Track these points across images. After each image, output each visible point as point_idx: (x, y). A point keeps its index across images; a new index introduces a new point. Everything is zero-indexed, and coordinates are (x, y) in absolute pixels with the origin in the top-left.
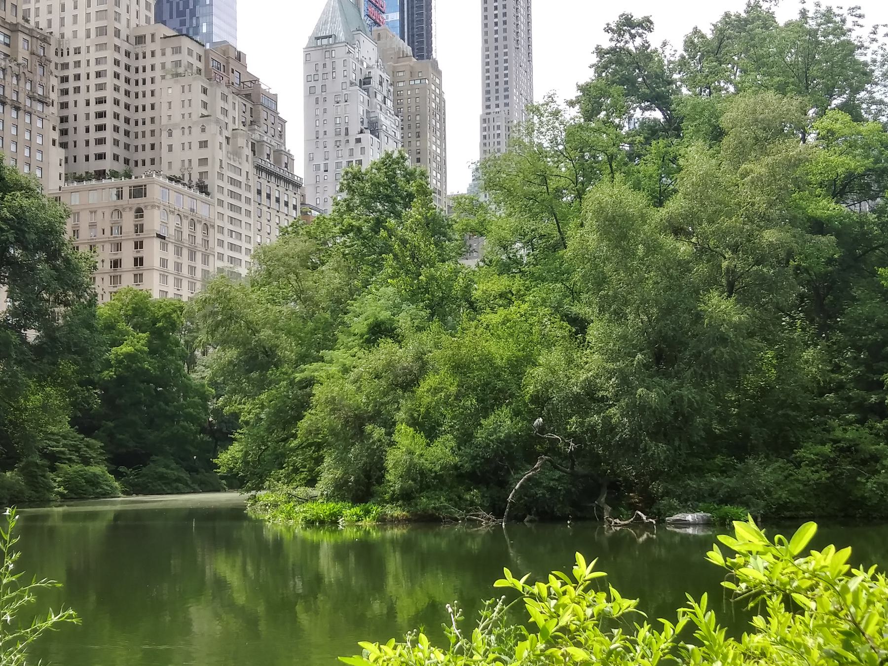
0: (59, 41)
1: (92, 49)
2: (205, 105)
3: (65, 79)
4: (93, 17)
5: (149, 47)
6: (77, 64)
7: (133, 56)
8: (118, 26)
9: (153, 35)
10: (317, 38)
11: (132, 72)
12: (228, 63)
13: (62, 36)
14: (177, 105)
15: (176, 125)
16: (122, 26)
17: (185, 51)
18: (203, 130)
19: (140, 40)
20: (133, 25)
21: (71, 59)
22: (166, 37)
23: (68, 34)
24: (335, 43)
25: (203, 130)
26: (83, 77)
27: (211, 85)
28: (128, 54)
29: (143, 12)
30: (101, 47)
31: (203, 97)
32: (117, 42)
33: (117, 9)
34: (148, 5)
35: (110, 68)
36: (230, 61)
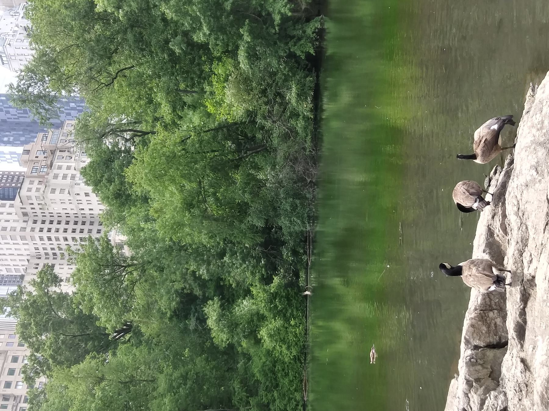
0: (32, 257)
1: (35, 242)
2: (62, 191)
3: (55, 254)
4: (15, 242)
5: (28, 209)
6: (44, 249)
7: (36, 218)
8: (18, 229)
9: (21, 208)
10: (3, 64)
11: (47, 221)
12: (32, 161)
13: (28, 255)
14: (64, 206)
15: (77, 207)
16: (19, 225)
17: (29, 194)
18: (78, 194)
19: (25, 214)
20: (16, 217)
21: (42, 252)
22: (21, 202)
23: (28, 253)
24: (5, 53)
25: (78, 194)
26: (52, 246)
27: (49, 186)
28: (35, 222)
29: (7, 209)
30: (33, 238)
31: (57, 192)
32: (28, 229)
33: (8, 229)
34: (4, 206)
35: (45, 235)
36: (30, 159)
